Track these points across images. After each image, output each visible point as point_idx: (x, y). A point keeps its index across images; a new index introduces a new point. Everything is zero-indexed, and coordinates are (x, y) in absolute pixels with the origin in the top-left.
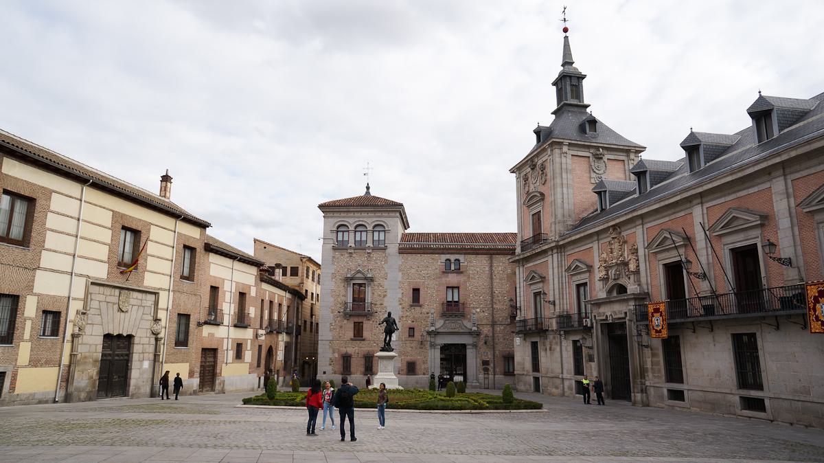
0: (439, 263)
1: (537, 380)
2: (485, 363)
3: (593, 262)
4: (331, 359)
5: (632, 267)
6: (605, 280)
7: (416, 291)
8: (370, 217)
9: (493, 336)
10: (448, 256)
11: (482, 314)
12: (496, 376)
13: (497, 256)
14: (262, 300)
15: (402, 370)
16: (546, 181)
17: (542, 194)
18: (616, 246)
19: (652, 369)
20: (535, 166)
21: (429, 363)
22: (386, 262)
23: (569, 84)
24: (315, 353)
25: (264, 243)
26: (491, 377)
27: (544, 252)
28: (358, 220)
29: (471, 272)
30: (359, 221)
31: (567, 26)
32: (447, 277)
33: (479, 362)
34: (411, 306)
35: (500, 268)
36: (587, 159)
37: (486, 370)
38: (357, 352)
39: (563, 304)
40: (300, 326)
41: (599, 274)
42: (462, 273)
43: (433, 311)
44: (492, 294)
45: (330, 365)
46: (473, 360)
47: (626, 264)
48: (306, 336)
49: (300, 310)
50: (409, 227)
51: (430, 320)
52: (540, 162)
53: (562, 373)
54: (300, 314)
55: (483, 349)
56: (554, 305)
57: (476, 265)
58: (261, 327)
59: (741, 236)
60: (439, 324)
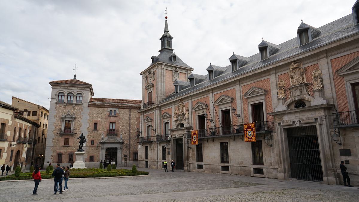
0: (107, 112)
1: (147, 162)
2: (125, 156)
3: (172, 114)
4: (52, 156)
5: (186, 116)
6: (176, 121)
7: (96, 124)
8: (75, 89)
9: (129, 144)
10: (111, 109)
11: (125, 135)
12: (130, 161)
13: (133, 110)
14: (15, 127)
15: (87, 160)
16: (155, 79)
17: (153, 85)
18: (181, 108)
19: (192, 157)
20: (151, 72)
21: (100, 156)
22: (82, 110)
23: (166, 40)
24: (44, 153)
25: (18, 99)
26: (128, 162)
27: (153, 109)
28: (69, 90)
30: (70, 91)
31: (167, 16)
32: (110, 118)
33: (123, 155)
34: (93, 131)
36: (171, 71)
37: (126, 159)
38: (65, 152)
39: (159, 131)
40: (36, 140)
41: (174, 119)
42: (117, 116)
43: (103, 133)
45: (51, 158)
46: (120, 155)
47: (184, 115)
48: (39, 145)
49: (37, 132)
50: (94, 95)
51: (101, 137)
52: (153, 71)
53: (157, 159)
54: (36, 134)
55: (125, 150)
56: (156, 131)
57: (123, 113)
58: (14, 141)
59: (225, 106)
60: (106, 139)
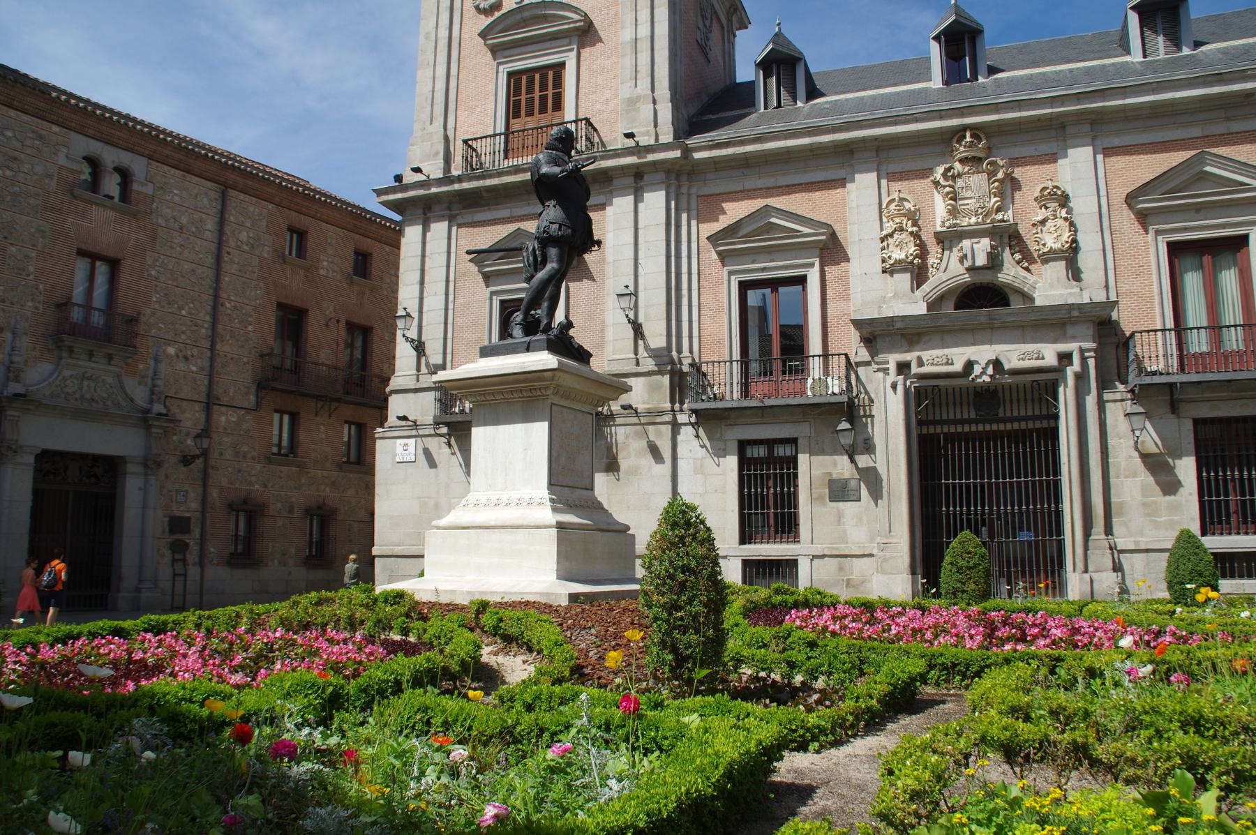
2: (178, 525)
10: (95, 148)
11: (181, 365)
13: (242, 196)
26: (194, 572)
29: (161, 222)
35: (244, 236)
37: (179, 548)
44: (215, 309)
